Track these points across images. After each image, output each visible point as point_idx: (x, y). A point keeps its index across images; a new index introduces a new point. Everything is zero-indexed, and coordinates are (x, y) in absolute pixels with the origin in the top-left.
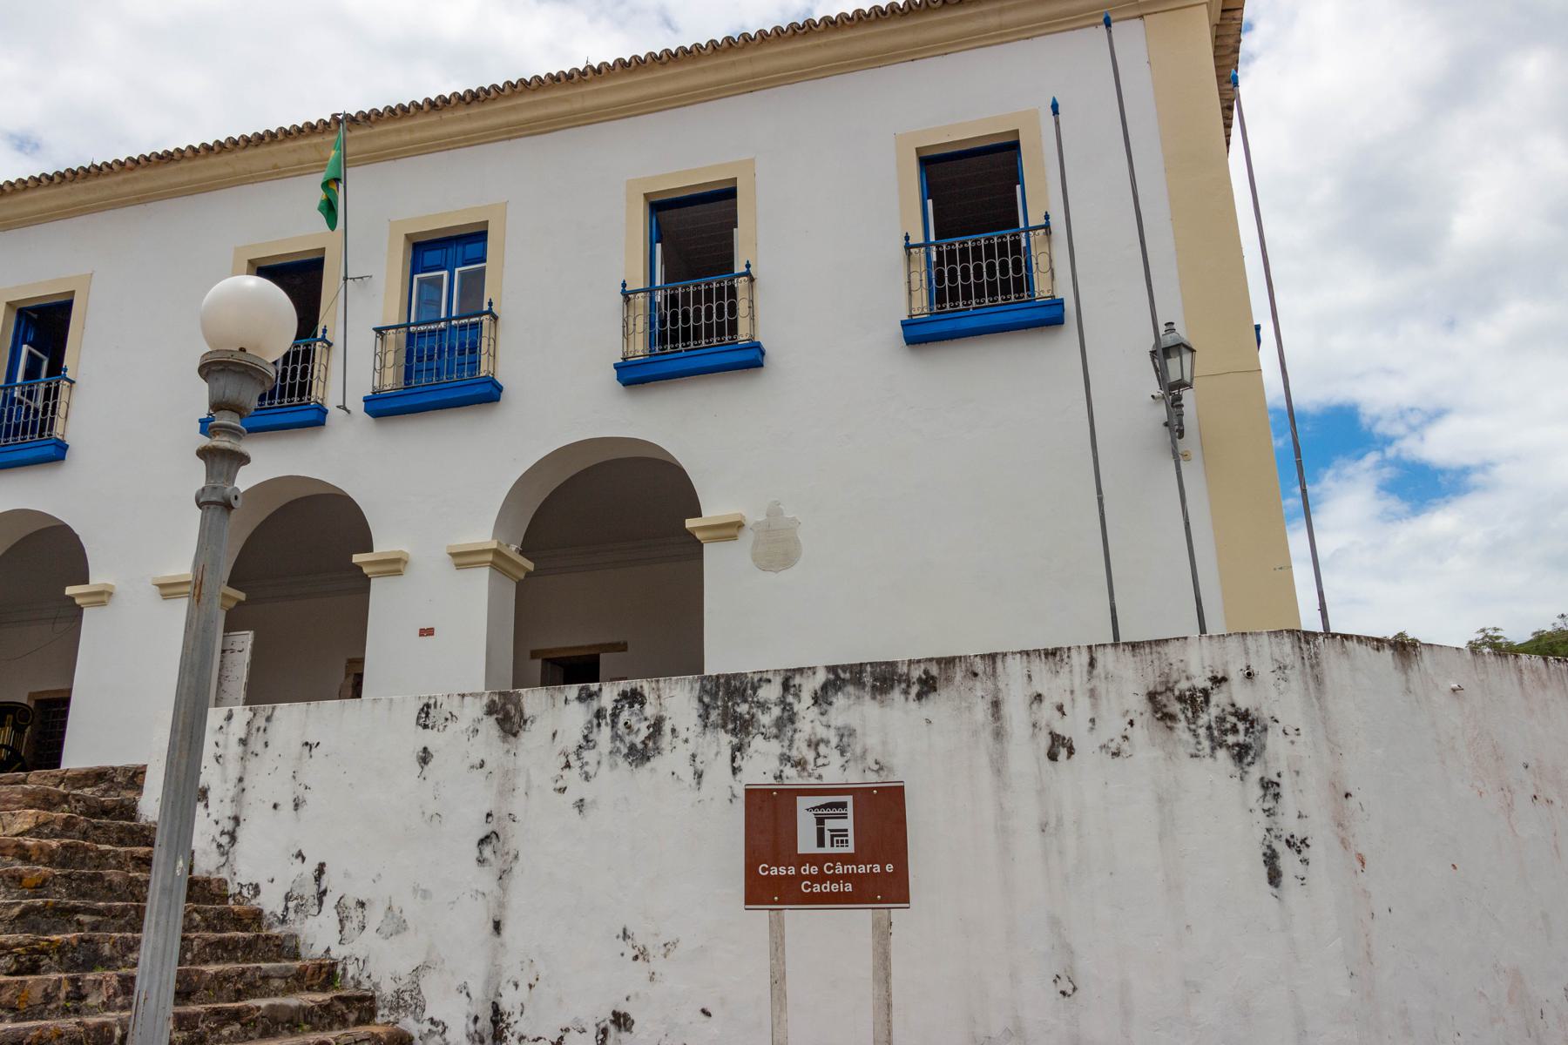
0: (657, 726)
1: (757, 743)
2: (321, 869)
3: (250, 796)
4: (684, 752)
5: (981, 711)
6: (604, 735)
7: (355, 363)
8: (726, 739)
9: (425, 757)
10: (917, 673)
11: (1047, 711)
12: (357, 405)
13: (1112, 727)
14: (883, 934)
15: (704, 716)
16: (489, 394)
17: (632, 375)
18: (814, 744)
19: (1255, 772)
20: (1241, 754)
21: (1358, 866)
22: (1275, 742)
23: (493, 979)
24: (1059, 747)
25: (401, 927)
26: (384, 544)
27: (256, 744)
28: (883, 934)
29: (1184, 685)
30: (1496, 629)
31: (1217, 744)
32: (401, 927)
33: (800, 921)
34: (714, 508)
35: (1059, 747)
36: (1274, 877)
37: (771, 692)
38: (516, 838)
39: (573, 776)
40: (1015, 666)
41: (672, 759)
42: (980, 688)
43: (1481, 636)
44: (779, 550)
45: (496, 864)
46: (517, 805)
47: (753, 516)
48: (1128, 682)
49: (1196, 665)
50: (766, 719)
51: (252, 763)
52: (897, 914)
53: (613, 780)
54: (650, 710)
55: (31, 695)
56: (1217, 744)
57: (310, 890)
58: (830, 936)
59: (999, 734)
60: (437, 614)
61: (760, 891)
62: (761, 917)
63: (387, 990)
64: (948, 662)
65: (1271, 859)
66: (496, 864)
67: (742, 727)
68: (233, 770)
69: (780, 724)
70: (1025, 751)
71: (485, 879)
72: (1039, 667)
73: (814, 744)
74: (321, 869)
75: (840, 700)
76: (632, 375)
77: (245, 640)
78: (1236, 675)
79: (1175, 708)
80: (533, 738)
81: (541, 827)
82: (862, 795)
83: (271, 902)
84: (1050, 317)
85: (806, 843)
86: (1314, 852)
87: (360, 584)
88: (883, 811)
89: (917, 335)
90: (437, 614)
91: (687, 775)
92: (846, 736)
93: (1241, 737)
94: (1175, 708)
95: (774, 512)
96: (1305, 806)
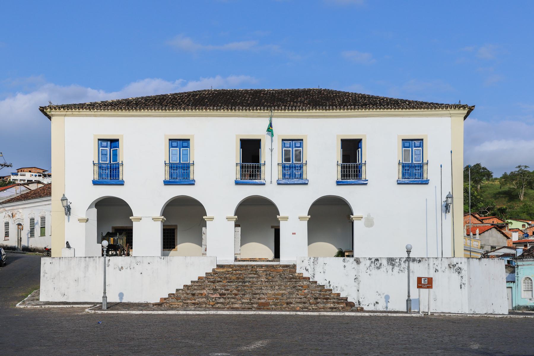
0: (381, 264)
1: (396, 267)
2: (329, 282)
3: (316, 271)
5: (427, 265)
6: (373, 264)
8: (391, 267)
9: (345, 267)
10: (418, 259)
11: (435, 265)
13: (443, 268)
14: (429, 291)
15: (388, 263)
19: (460, 275)
20: (459, 272)
22: (463, 272)
23: (358, 297)
24: (436, 270)
27: (316, 263)
28: (429, 291)
30: (526, 167)
31: (456, 271)
33: (421, 289)
34: (356, 213)
36: (461, 288)
37: (398, 261)
38: (360, 279)
39: (368, 271)
40: (431, 259)
41: (383, 269)
43: (518, 169)
44: (370, 223)
45: (358, 282)
46: (360, 274)
47: (364, 216)
48: (446, 263)
49: (455, 261)
50: (397, 264)
51: (315, 266)
52: (431, 289)
53: (374, 271)
54: (380, 262)
55: (113, 228)
56: (456, 271)
58: (424, 291)
59: (429, 268)
61: (419, 287)
64: (423, 258)
65: (461, 286)
66: (358, 282)
68: (312, 267)
69: (399, 265)
71: (356, 284)
72: (435, 260)
74: (329, 282)
76: (338, 183)
78: (459, 263)
80: (362, 265)
81: (364, 277)
82: (428, 278)
84: (426, 183)
85: (423, 283)
86: (466, 285)
91: (385, 271)
93: (459, 271)
95: (369, 215)
96: (465, 280)
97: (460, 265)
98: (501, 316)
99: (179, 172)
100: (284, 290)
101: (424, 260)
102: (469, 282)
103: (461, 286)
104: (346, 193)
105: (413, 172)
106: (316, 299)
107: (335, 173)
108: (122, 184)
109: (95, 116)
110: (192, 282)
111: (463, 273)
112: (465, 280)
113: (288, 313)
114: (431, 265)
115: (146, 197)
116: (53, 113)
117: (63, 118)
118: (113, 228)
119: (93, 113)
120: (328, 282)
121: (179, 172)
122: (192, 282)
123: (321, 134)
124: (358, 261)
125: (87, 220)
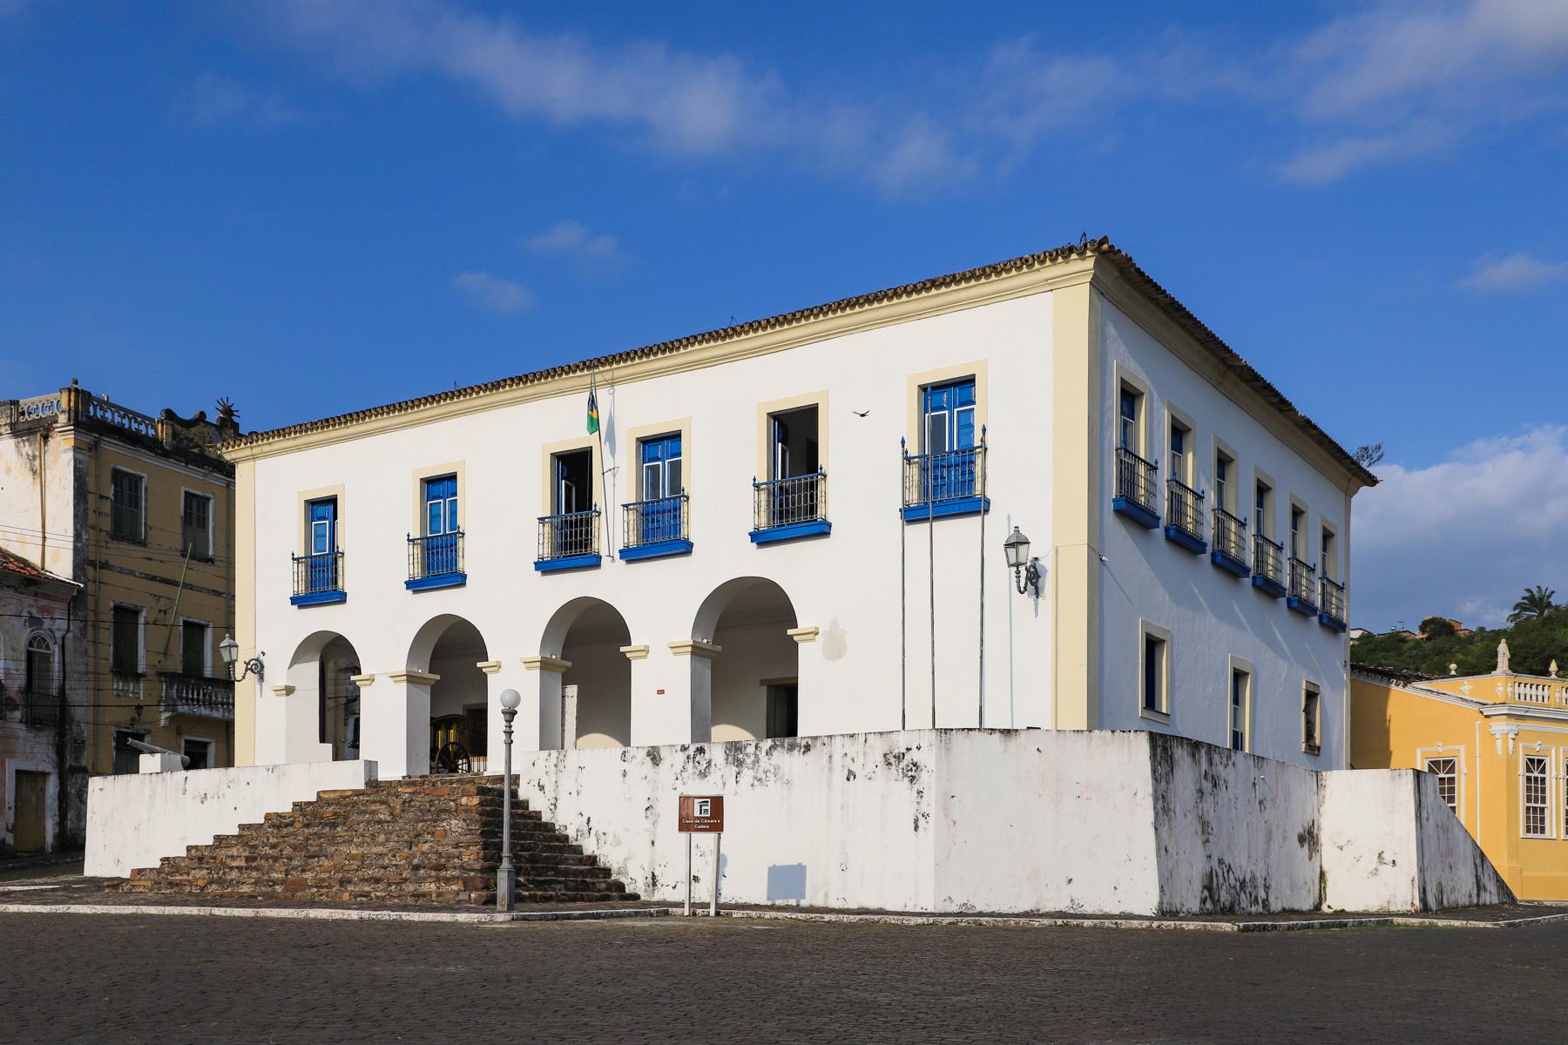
0: (709, 763)
1: (745, 771)
4: (719, 774)
5: (826, 758)
7: (613, 527)
8: (734, 769)
11: (848, 759)
12: (617, 555)
16: (686, 548)
17: (761, 539)
18: (766, 772)
19: (916, 787)
21: (922, 822)
24: (851, 775)
25: (619, 843)
26: (637, 640)
27: (561, 766)
29: (896, 752)
32: (619, 843)
33: (694, 835)
35: (851, 775)
36: (916, 828)
40: (839, 740)
42: (826, 749)
48: (878, 748)
50: (749, 761)
54: (707, 756)
55: (465, 707)
57: (586, 828)
58: (705, 840)
59: (830, 770)
60: (662, 681)
62: (685, 835)
63: (615, 868)
64: (815, 738)
65: (916, 821)
66: (652, 818)
67: (740, 763)
70: (840, 776)
71: (648, 824)
72: (847, 740)
73: (766, 772)
75: (775, 753)
76: (761, 539)
77: (572, 690)
79: (892, 760)
80: (664, 766)
82: (712, 798)
83: (571, 833)
87: (625, 664)
88: (717, 803)
89: (911, 515)
90: (662, 681)
91: (720, 783)
92: (777, 768)
93: (912, 773)
94: (892, 760)
96: (930, 803)
97: (914, 755)
98: (920, 920)
99: (439, 562)
100: (383, 844)
101: (819, 743)
102: (945, 808)
103: (916, 821)
104: (785, 566)
105: (946, 482)
106: (416, 868)
107: (749, 511)
108: (341, 598)
109: (299, 448)
110: (240, 826)
111: (925, 779)
112: (930, 803)
113: (354, 915)
114: (837, 759)
115: (383, 620)
116: (234, 455)
117: (251, 463)
118: (465, 707)
119: (291, 443)
120: (585, 819)
121: (439, 562)
122: (240, 826)
123: (717, 406)
124: (654, 756)
125: (289, 690)
